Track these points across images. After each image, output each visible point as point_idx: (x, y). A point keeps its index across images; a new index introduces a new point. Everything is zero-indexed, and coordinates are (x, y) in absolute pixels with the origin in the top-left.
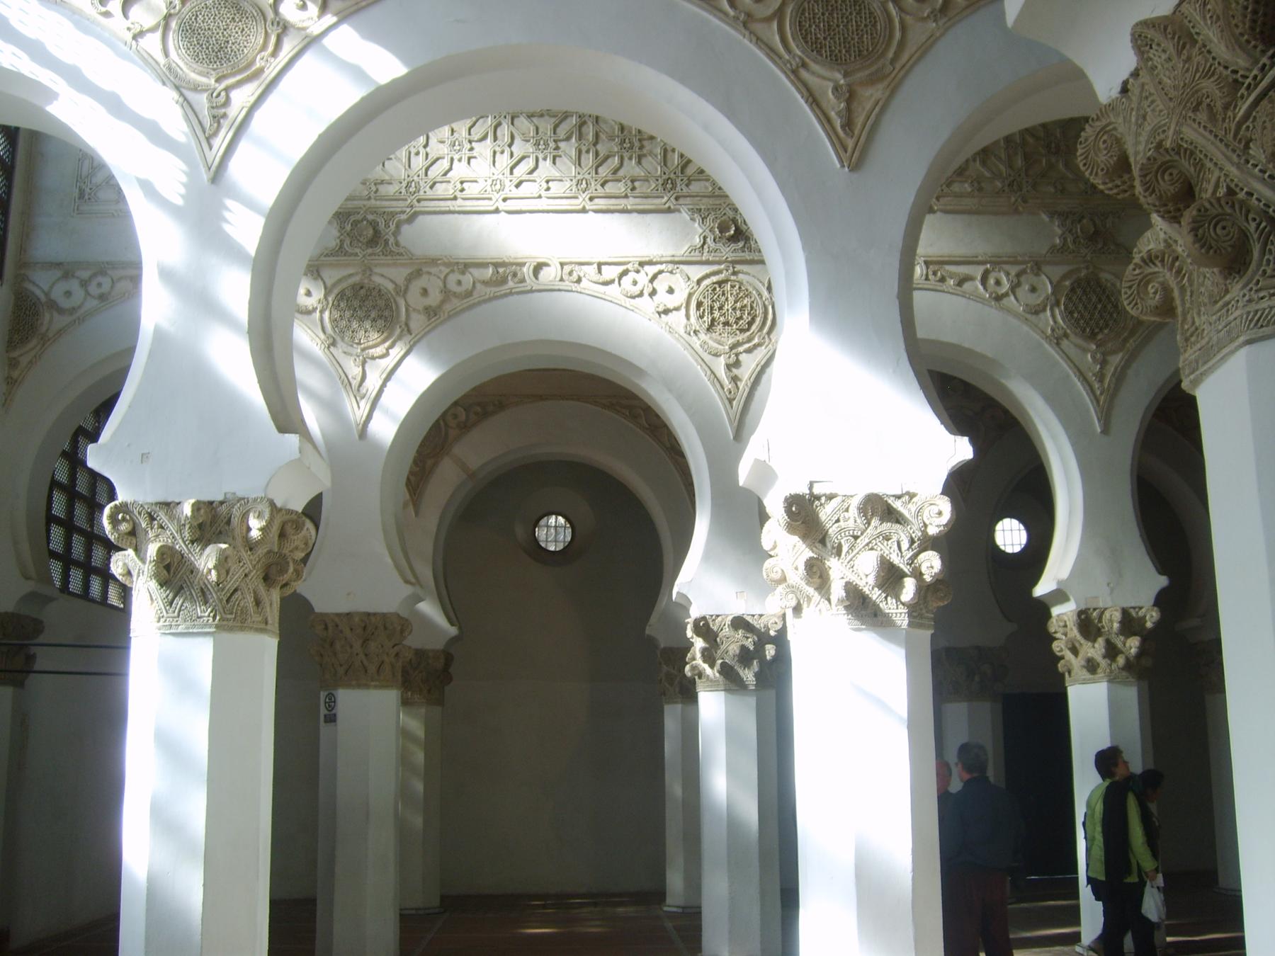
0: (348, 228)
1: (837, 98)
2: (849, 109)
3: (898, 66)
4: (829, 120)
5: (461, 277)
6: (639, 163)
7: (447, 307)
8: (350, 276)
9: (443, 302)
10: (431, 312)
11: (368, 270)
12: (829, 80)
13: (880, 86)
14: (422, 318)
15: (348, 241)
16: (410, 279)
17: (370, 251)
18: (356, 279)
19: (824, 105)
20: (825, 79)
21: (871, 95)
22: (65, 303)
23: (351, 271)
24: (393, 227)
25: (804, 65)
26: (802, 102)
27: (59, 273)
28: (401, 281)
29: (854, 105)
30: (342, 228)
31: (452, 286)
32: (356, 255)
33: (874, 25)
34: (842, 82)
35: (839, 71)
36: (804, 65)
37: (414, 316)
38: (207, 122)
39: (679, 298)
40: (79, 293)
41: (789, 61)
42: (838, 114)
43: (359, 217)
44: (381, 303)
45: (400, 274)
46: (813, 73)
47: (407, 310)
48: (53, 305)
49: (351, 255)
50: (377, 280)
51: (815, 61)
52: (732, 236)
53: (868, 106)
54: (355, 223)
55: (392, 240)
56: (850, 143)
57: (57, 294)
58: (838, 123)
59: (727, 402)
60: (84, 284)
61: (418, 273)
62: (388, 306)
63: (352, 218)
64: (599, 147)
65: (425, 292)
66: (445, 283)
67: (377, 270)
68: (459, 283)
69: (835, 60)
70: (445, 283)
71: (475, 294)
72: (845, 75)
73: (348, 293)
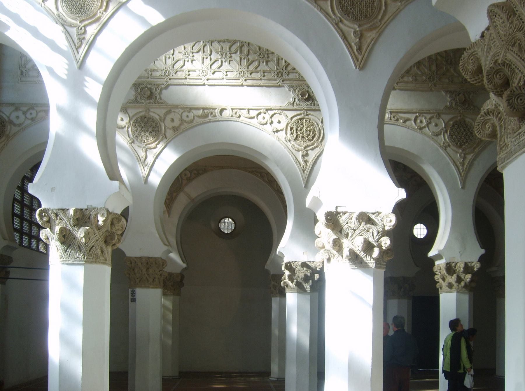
0: (139, 91)
1: (355, 37)
2: (360, 42)
3: (383, 22)
4: (351, 47)
5: (188, 114)
6: (267, 64)
7: (182, 127)
8: (140, 112)
9: (181, 125)
10: (175, 129)
11: (148, 110)
12: (352, 28)
13: (374, 32)
15: (139, 97)
16: (166, 114)
17: (148, 101)
18: (143, 114)
19: (349, 40)
20: (350, 28)
21: (370, 35)
22: (17, 122)
24: (158, 91)
25: (341, 21)
26: (340, 38)
27: (13, 108)
29: (363, 40)
30: (136, 91)
31: (184, 118)
32: (143, 103)
33: (373, 3)
34: (358, 29)
35: (356, 24)
36: (341, 21)
37: (168, 130)
38: (76, 41)
40: (22, 117)
41: (334, 19)
42: (355, 44)
43: (144, 86)
44: (154, 125)
45: (161, 112)
46: (345, 25)
47: (165, 128)
48: (11, 122)
49: (140, 103)
50: (152, 114)
51: (346, 19)
52: (307, 99)
53: (369, 40)
54: (142, 89)
55: (158, 97)
56: (360, 58)
57: (13, 117)
58: (355, 48)
60: (25, 113)
61: (170, 112)
62: (156, 126)
63: (141, 86)
64: (249, 57)
65: (173, 120)
67: (152, 110)
68: (188, 116)
69: (355, 19)
71: (195, 122)
72: (359, 26)
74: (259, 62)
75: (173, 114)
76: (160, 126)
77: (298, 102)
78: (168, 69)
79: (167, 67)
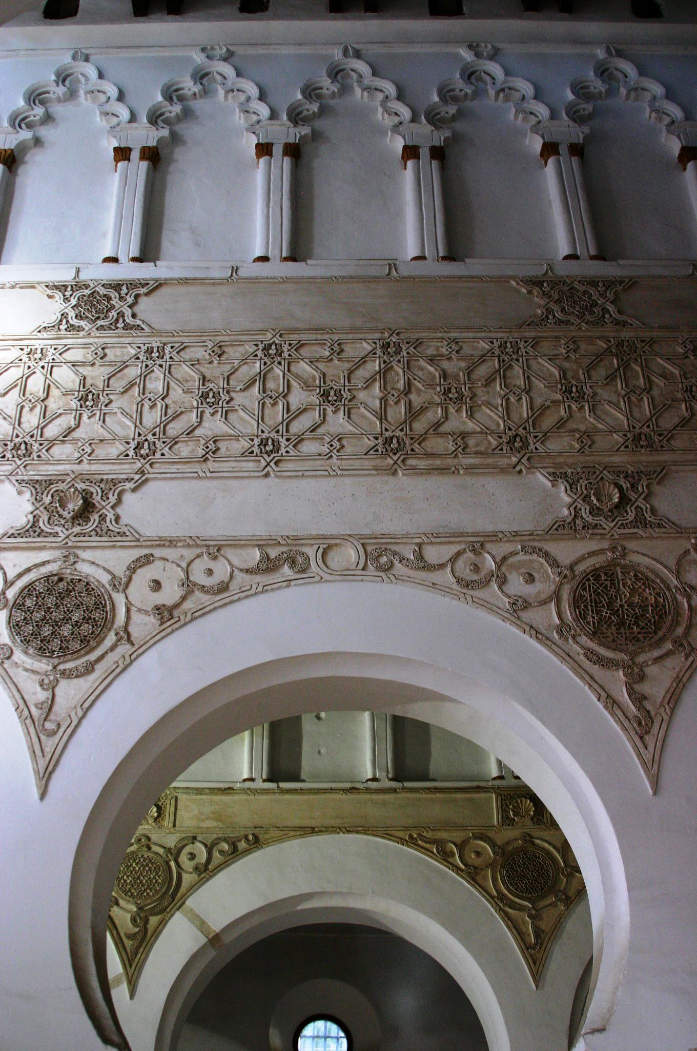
5: (212, 565)
6: (471, 416)
7: (188, 605)
9: (184, 598)
11: (70, 556)
15: (45, 517)
16: (133, 568)
17: (77, 529)
23: (45, 556)
24: (113, 499)
28: (120, 571)
31: (198, 576)
32: (56, 535)
37: (136, 617)
39: (542, 588)
44: (90, 601)
45: (118, 559)
47: (128, 611)
50: (84, 569)
52: (617, 506)
55: (110, 516)
59: (637, 740)
61: (147, 560)
62: (99, 605)
63: (54, 488)
64: (413, 397)
65: (157, 585)
66: (187, 573)
68: (210, 572)
70: (187, 573)
71: (233, 587)
74: (446, 411)
75: (159, 564)
76: (113, 604)
77: (590, 519)
78: (150, 437)
79: (143, 431)
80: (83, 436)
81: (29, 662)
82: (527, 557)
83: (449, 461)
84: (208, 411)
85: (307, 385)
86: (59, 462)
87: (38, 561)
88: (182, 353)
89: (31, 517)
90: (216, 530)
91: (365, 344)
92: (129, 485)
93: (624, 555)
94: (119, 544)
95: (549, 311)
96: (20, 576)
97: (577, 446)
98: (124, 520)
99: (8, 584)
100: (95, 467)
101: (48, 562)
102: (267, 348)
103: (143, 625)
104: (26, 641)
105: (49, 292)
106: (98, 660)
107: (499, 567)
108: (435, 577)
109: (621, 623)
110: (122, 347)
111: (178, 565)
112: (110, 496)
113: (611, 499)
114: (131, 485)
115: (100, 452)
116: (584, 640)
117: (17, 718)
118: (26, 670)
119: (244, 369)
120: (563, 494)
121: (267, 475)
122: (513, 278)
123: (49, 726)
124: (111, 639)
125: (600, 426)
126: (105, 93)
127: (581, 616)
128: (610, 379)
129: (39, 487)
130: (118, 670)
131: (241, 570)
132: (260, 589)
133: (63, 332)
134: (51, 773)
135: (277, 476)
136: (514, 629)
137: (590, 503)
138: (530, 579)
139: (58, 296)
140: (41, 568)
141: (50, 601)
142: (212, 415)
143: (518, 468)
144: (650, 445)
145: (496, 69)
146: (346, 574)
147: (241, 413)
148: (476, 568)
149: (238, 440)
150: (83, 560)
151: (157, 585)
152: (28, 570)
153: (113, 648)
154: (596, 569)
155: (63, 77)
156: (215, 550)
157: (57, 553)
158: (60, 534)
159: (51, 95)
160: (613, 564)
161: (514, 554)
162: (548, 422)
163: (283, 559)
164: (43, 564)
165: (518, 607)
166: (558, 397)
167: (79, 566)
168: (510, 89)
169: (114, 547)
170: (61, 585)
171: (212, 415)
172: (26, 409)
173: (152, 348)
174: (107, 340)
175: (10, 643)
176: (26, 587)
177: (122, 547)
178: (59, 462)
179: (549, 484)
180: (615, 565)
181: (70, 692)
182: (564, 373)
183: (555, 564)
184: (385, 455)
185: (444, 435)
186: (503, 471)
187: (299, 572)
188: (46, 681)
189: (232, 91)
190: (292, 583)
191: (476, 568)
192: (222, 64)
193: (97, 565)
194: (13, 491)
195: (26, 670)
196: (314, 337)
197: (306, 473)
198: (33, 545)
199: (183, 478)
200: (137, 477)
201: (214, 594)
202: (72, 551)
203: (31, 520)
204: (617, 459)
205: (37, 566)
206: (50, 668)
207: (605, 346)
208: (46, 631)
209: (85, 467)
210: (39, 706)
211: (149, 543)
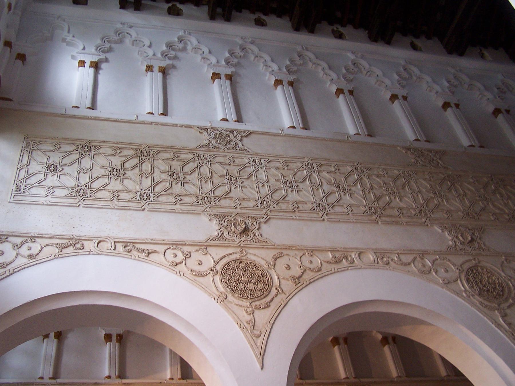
5: (311, 259)
6: (401, 200)
7: (305, 276)
14: (290, 282)
16: (276, 258)
17: (243, 239)
18: (237, 256)
24: (257, 226)
37: (283, 282)
50: (253, 258)
60: (17, 247)
62: (264, 275)
65: (288, 268)
67: (250, 251)
71: (323, 268)
73: (232, 265)
74: (390, 197)
75: (286, 257)
77: (461, 246)
80: (234, 196)
81: (236, 301)
82: (442, 261)
83: (398, 219)
84: (289, 190)
85: (330, 183)
86: (226, 207)
87: (227, 253)
88: (269, 163)
89: (219, 231)
90: (308, 242)
91: (348, 167)
92: (263, 220)
93: (479, 262)
94: (265, 247)
95: (417, 161)
96: (221, 259)
97: (446, 216)
98: (264, 235)
99: (216, 263)
100: (243, 211)
101: (233, 253)
102: (307, 165)
103: (288, 286)
104: (232, 290)
105: (200, 131)
106: (272, 300)
107: (433, 265)
108: (407, 268)
109: (488, 291)
110: (241, 158)
111: (296, 258)
112: (255, 224)
113: (467, 239)
114: (263, 220)
115: (245, 204)
116: (477, 297)
117: (239, 329)
118: (237, 305)
119: (299, 173)
120: (447, 235)
121: (324, 220)
122: (398, 146)
123: (257, 332)
124: (274, 291)
125: (452, 209)
126: (201, 49)
127: (472, 287)
128: (449, 189)
129: (221, 217)
130: (282, 306)
131: (325, 262)
132: (336, 270)
133: (212, 149)
134: (263, 356)
135: (328, 221)
136: (447, 292)
137: (459, 240)
138: (447, 271)
139: (205, 133)
140: (230, 256)
141: (239, 272)
142: (291, 191)
143: (426, 224)
144: (474, 217)
145: (364, 63)
146: (371, 266)
147: (304, 192)
148: (424, 266)
149: (306, 204)
150: (250, 254)
151: (288, 268)
152: (224, 257)
153: (276, 295)
154: (471, 267)
155: (181, 40)
156: (312, 252)
157: (237, 250)
158: (236, 240)
159: (176, 47)
160: (476, 266)
161: (437, 259)
162: (431, 206)
163: (341, 258)
164: (231, 254)
165: (447, 283)
166: (432, 195)
167: (248, 256)
168: (372, 71)
169: (263, 248)
170: (243, 264)
171: (291, 191)
172: (203, 182)
173: (255, 160)
174: (234, 154)
175: (225, 291)
176: (225, 265)
177: (267, 248)
178: (226, 207)
179: (440, 231)
180: (477, 266)
181: (262, 317)
182: (431, 185)
183: (455, 265)
184: (371, 215)
185: (392, 208)
186: (421, 225)
187: (350, 263)
188: (248, 310)
189: (257, 57)
190: (349, 268)
191: (424, 266)
192: (251, 45)
193: (258, 256)
194: (207, 219)
195: (237, 305)
196: (326, 162)
197: (341, 220)
198: (224, 245)
199: (287, 219)
200: (265, 217)
201: (316, 272)
202: (243, 249)
203: (220, 233)
204: (463, 222)
205: (228, 255)
206: (248, 304)
207: (443, 177)
208: (241, 286)
209: (238, 210)
210: (248, 323)
211: (280, 247)
